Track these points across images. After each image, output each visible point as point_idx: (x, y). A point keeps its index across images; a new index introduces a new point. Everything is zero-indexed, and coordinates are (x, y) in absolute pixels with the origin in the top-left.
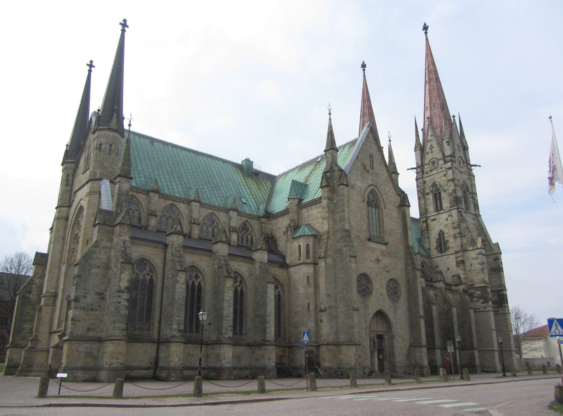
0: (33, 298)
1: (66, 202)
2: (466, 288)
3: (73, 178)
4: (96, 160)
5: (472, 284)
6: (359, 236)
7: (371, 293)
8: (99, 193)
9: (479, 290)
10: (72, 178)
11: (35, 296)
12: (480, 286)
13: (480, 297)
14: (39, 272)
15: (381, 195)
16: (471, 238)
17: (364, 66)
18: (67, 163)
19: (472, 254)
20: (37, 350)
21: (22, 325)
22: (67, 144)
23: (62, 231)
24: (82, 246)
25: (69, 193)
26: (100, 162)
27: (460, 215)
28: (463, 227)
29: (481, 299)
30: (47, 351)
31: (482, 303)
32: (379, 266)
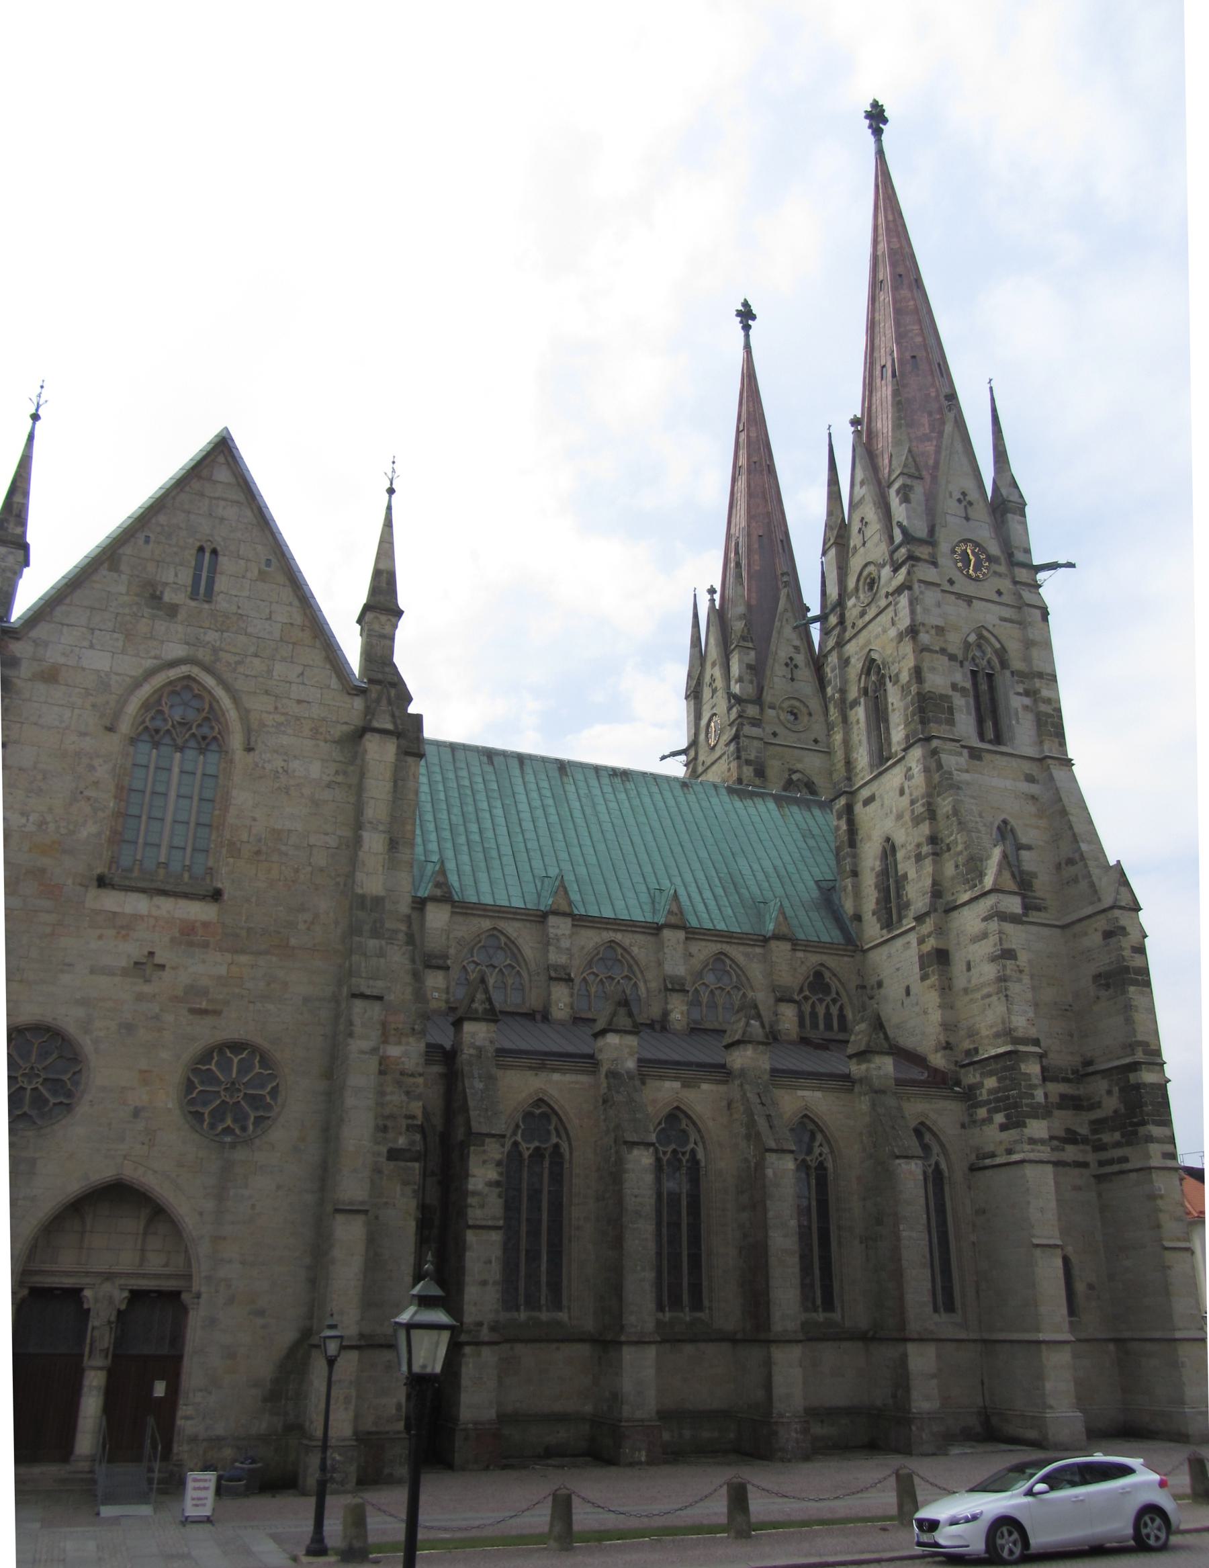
2: (952, 1067)
5: (972, 1046)
6: (43, 871)
7: (69, 1108)
9: (991, 1074)
12: (993, 1052)
13: (1001, 1102)
15: (236, 700)
16: (965, 853)
17: (746, 315)
19: (970, 920)
27: (934, 766)
28: (945, 810)
29: (997, 1110)
31: (1003, 1128)
32: (147, 989)
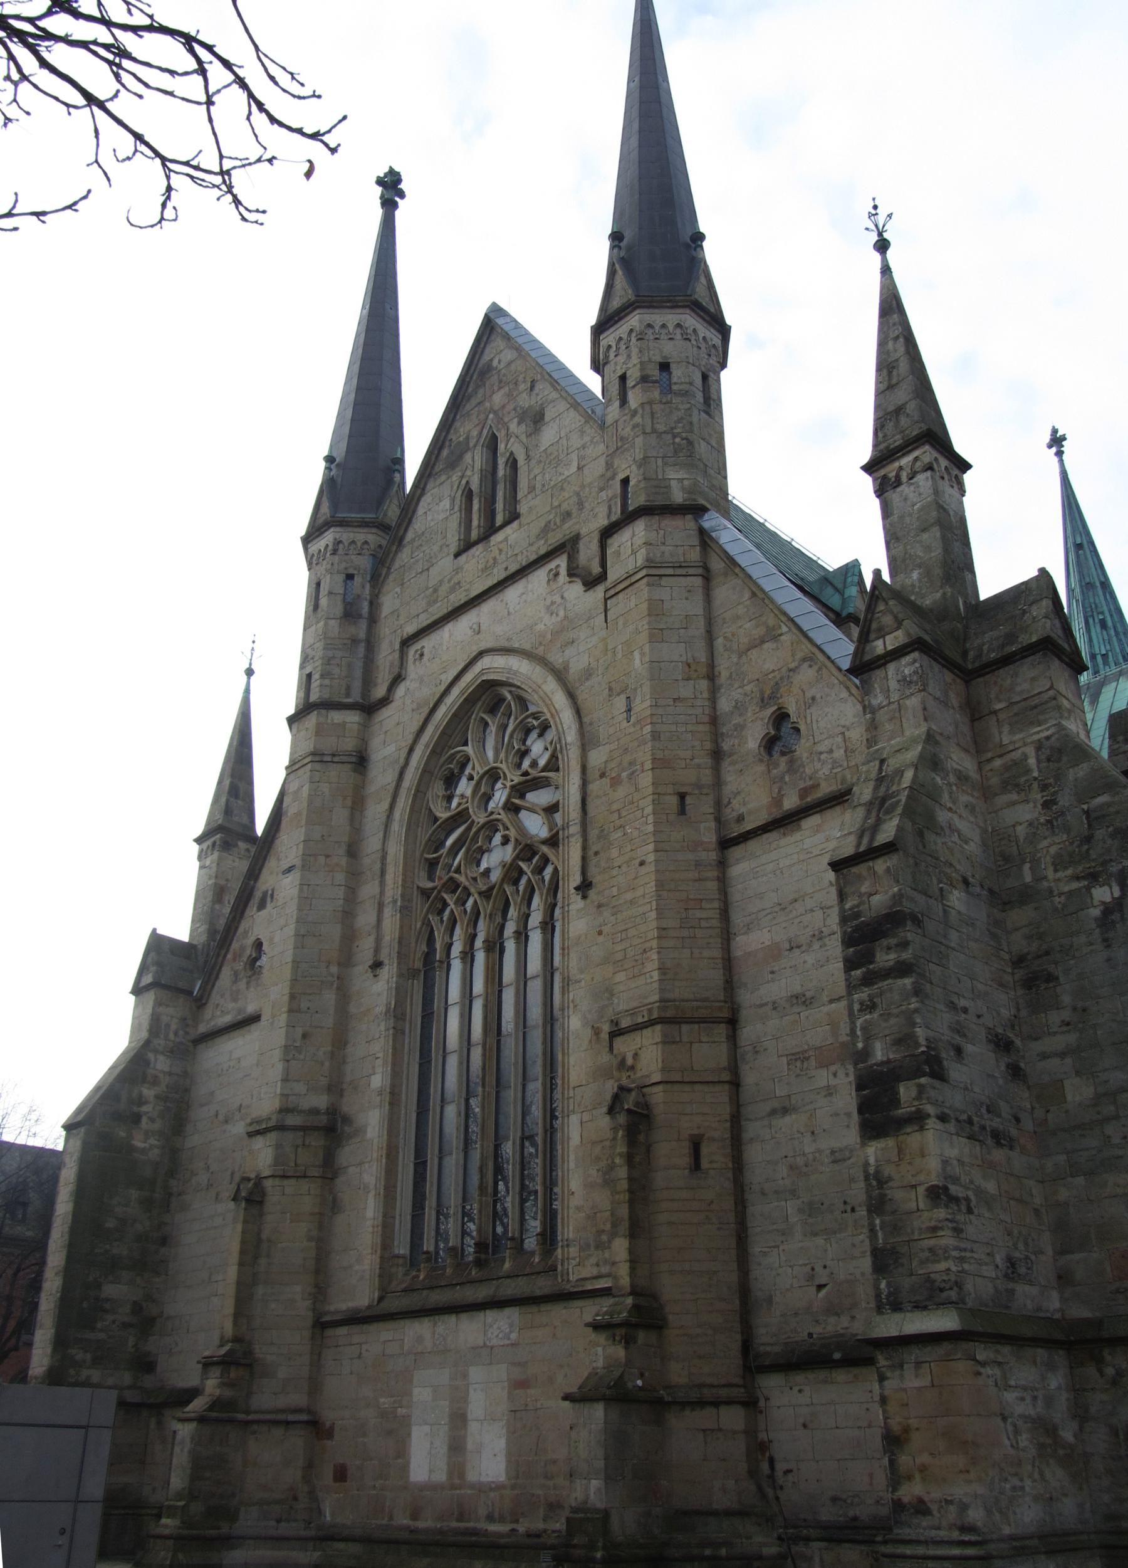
0: (143, 1151)
1: (348, 688)
3: (373, 587)
4: (654, 431)
8: (700, 571)
10: (368, 586)
11: (153, 1141)
14: (168, 1026)
18: (342, 523)
20: (250, 1417)
21: (98, 1286)
22: (326, 453)
23: (340, 816)
24: (655, 823)
25: (361, 650)
26: (674, 437)
30: (307, 1422)
